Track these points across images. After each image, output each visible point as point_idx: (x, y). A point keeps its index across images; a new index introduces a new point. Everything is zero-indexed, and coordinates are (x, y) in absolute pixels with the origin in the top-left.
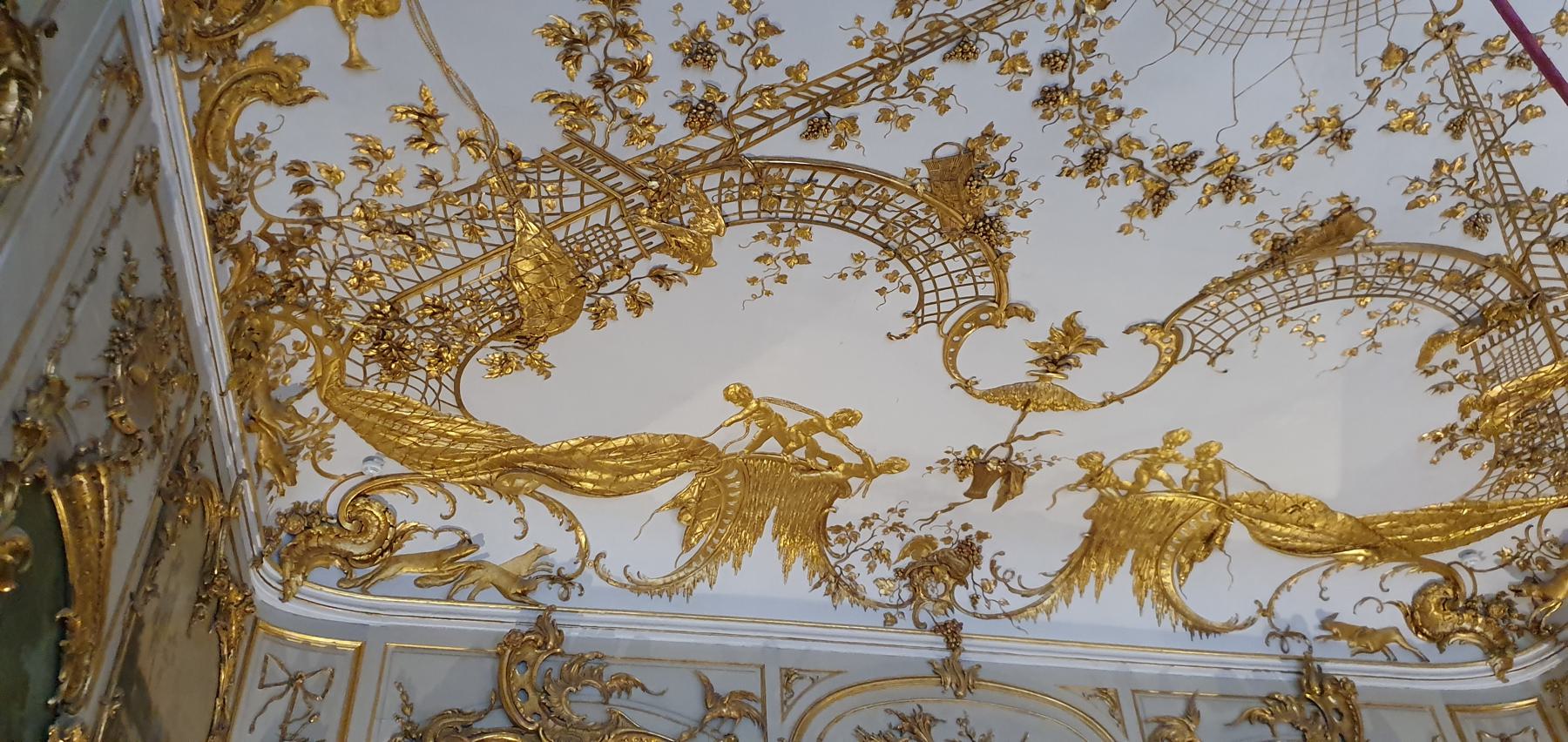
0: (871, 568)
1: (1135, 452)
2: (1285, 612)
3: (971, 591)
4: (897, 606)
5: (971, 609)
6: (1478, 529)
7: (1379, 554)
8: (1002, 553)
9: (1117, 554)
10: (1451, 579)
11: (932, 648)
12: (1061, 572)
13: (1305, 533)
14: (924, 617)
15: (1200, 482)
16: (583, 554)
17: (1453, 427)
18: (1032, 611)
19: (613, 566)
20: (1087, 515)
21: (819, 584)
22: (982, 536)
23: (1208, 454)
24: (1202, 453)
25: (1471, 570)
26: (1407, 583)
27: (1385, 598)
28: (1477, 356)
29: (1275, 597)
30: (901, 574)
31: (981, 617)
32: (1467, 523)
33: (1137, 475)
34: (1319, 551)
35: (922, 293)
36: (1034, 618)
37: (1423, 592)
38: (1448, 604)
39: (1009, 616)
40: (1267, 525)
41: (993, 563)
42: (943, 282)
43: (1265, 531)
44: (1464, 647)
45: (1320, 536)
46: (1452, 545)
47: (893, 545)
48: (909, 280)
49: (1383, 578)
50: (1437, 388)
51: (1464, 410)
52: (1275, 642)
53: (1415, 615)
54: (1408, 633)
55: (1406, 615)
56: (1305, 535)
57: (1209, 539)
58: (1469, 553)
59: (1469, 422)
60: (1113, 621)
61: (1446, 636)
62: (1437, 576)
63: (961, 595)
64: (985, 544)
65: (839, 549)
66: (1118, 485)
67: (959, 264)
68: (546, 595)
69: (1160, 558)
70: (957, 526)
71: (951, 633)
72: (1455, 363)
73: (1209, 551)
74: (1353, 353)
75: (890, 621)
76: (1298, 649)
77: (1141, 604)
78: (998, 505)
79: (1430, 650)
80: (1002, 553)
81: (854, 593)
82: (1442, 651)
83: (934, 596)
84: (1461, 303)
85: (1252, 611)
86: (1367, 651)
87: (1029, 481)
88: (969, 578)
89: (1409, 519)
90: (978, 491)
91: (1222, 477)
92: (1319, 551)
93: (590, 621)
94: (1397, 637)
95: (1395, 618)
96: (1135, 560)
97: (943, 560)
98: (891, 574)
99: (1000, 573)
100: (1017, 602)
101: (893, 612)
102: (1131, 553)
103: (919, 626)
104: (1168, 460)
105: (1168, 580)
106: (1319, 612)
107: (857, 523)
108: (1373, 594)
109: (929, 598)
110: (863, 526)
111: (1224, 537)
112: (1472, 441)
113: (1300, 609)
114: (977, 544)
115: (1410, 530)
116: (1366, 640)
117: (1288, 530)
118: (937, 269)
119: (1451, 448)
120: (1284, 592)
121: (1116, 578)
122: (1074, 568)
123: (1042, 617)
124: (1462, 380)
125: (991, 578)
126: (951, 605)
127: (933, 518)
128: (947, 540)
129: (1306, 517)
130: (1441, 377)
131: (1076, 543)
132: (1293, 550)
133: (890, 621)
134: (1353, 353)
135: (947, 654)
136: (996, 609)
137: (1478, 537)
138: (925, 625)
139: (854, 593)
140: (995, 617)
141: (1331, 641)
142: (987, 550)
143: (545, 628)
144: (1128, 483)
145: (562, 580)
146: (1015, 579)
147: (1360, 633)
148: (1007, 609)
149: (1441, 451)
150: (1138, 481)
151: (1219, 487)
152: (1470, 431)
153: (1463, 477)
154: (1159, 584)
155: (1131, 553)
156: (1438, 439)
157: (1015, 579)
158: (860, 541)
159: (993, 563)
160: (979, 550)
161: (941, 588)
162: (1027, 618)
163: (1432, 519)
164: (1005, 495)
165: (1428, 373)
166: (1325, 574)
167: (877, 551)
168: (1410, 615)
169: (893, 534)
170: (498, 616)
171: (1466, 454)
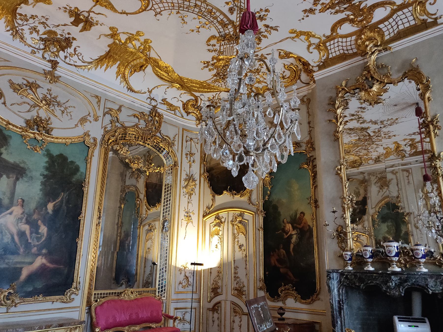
1: (127, 33)
2: (154, 94)
3: (65, 54)
4: (37, 49)
6: (206, 90)
7: (182, 87)
9: (115, 61)
10: (197, 101)
13: (166, 75)
14: (46, 55)
15: (143, 50)
17: (209, 62)
18: (84, 68)
20: (109, 46)
22: (74, 39)
23: (147, 42)
24: (146, 41)
25: (201, 99)
26: (186, 97)
27: (180, 99)
28: (220, 46)
29: (153, 89)
30: (42, 39)
31: (66, 63)
32: (204, 87)
33: (126, 40)
34: (168, 81)
36: (84, 70)
37: (189, 101)
38: (193, 106)
39: (76, 66)
40: (157, 69)
41: (75, 49)
43: (156, 70)
44: (192, 117)
45: (170, 78)
46: (199, 92)
47: (41, 29)
49: (181, 94)
50: (209, 50)
51: (213, 58)
52: (149, 100)
53: (185, 106)
54: (182, 109)
55: (183, 105)
56: (166, 75)
57: (141, 67)
58: (202, 95)
59: (213, 62)
60: (107, 79)
61: (190, 113)
62: (194, 98)
63: (62, 54)
64: (74, 42)
66: (120, 41)
69: (126, 67)
70: (66, 32)
71: (54, 64)
72: (215, 45)
73: (140, 70)
74: (193, 31)
75: (33, 52)
76: (154, 103)
77: (117, 77)
78: (81, 31)
79: (185, 115)
82: (187, 116)
83: (52, 51)
84: (222, 30)
85: (146, 90)
86: (170, 110)
87: (93, 28)
88: (66, 50)
89: (192, 82)
91: (149, 51)
92: (168, 81)
94: (179, 109)
95: (180, 105)
96: (119, 65)
97: (59, 41)
98: (38, 38)
99: (77, 53)
100: (79, 63)
101: (36, 50)
102: (119, 62)
103: (44, 58)
104: (136, 39)
105: (126, 73)
106: (163, 96)
108: (177, 97)
109: (50, 51)
111: (145, 68)
112: (212, 67)
113: (159, 94)
114: (72, 41)
115: (191, 84)
116: (171, 107)
117: (162, 72)
119: (207, 67)
120: (156, 88)
121: (112, 67)
122: (100, 61)
123: (86, 70)
124: (215, 51)
125: (73, 53)
128: (62, 35)
129: (168, 71)
130: (211, 48)
131: (103, 53)
132: (162, 78)
133: (33, 52)
134: (193, 31)
135: (51, 70)
136: (72, 62)
137: (205, 92)
138: (46, 58)
140: (71, 65)
141: (163, 105)
142: (75, 44)
144: (123, 41)
146: (81, 56)
147: (171, 105)
148: (76, 64)
149: (205, 67)
150: (126, 42)
151: (148, 53)
152: (212, 64)
153: (207, 76)
154: (124, 74)
155: (119, 62)
156: (205, 64)
157: (81, 56)
159: (75, 49)
160: (72, 43)
161: (55, 49)
163: (197, 84)
164: (84, 29)
165: (208, 45)
166: (168, 88)
167: (35, 28)
168: (184, 105)
171: (210, 70)
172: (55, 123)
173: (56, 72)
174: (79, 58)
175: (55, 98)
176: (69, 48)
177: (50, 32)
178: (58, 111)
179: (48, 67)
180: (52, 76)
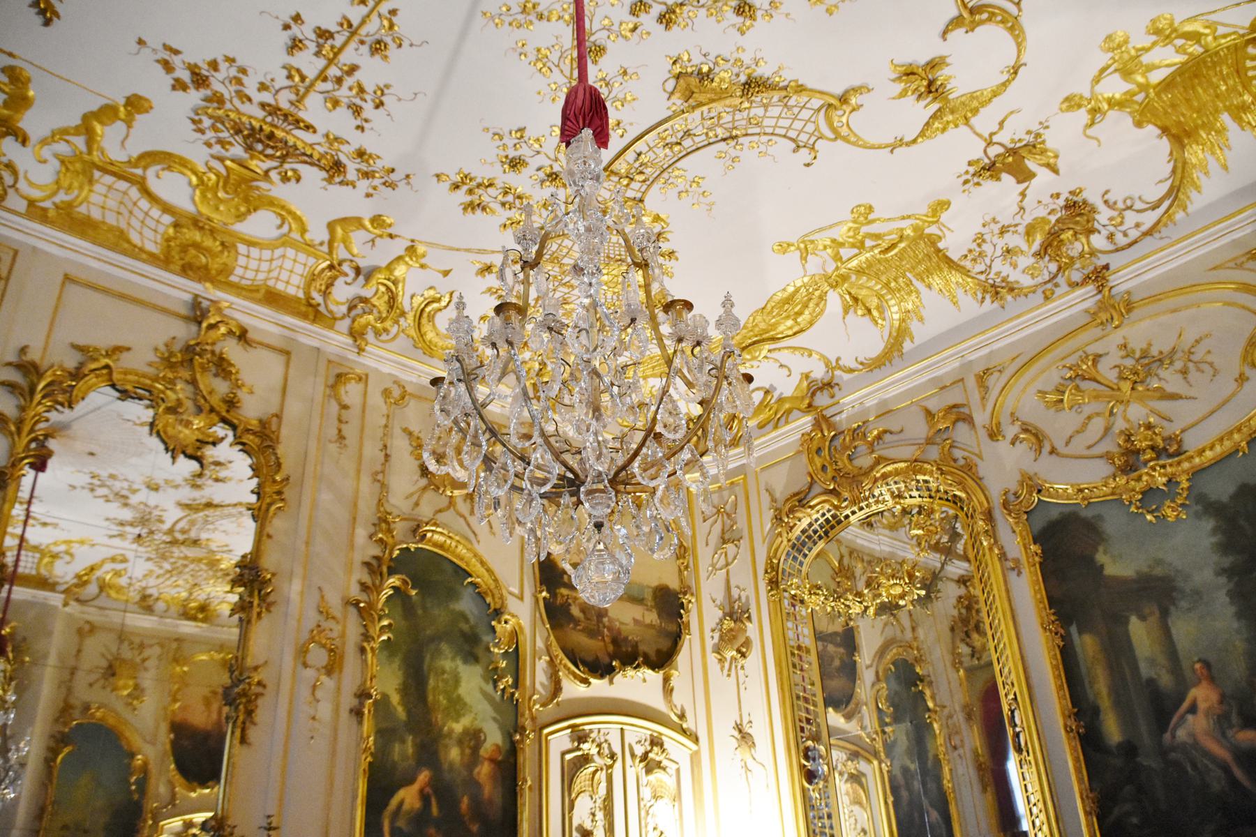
0: (1015, 266)
3: (1105, 232)
5: (1111, 247)
8: (1107, 192)
11: (1085, 298)
12: (1174, 171)
16: (827, 363)
19: (848, 362)
21: (983, 298)
31: (1123, 249)
35: (785, 136)
39: (1146, 234)
42: (786, 123)
47: (1014, 240)
48: (764, 139)
63: (1098, 241)
65: (980, 267)
67: (775, 111)
68: (822, 400)
70: (1046, 199)
71: (1099, 276)
80: (1107, 192)
81: (1012, 290)
88: (1096, 225)
90: (1024, 176)
93: (853, 403)
98: (1032, 260)
99: (1120, 205)
100: (1149, 219)
103: (1074, 285)
107: (974, 246)
110: (979, 245)
118: (766, 122)
123: (1180, 215)
125: (1115, 213)
126: (1093, 253)
127: (1022, 208)
131: (1165, 144)
135: (1099, 297)
136: (1134, 234)
139: (1012, 290)
140: (1135, 242)
142: (1093, 197)
143: (822, 421)
145: (828, 385)
158: (989, 255)
159: (1106, 202)
160: (1085, 202)
162: (1166, 225)
167: (1008, 251)
169: (1006, 235)
170: (804, 422)
172: (1180, 416)
173: (1114, 291)
174: (1138, 211)
175: (1145, 354)
176: (1097, 217)
177: (1030, 232)
178: (1169, 379)
179: (1085, 298)
180: (1114, 310)
